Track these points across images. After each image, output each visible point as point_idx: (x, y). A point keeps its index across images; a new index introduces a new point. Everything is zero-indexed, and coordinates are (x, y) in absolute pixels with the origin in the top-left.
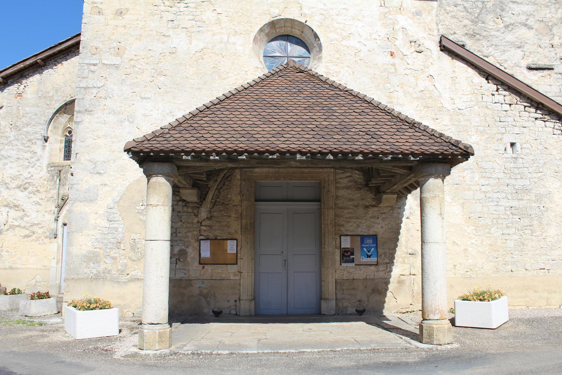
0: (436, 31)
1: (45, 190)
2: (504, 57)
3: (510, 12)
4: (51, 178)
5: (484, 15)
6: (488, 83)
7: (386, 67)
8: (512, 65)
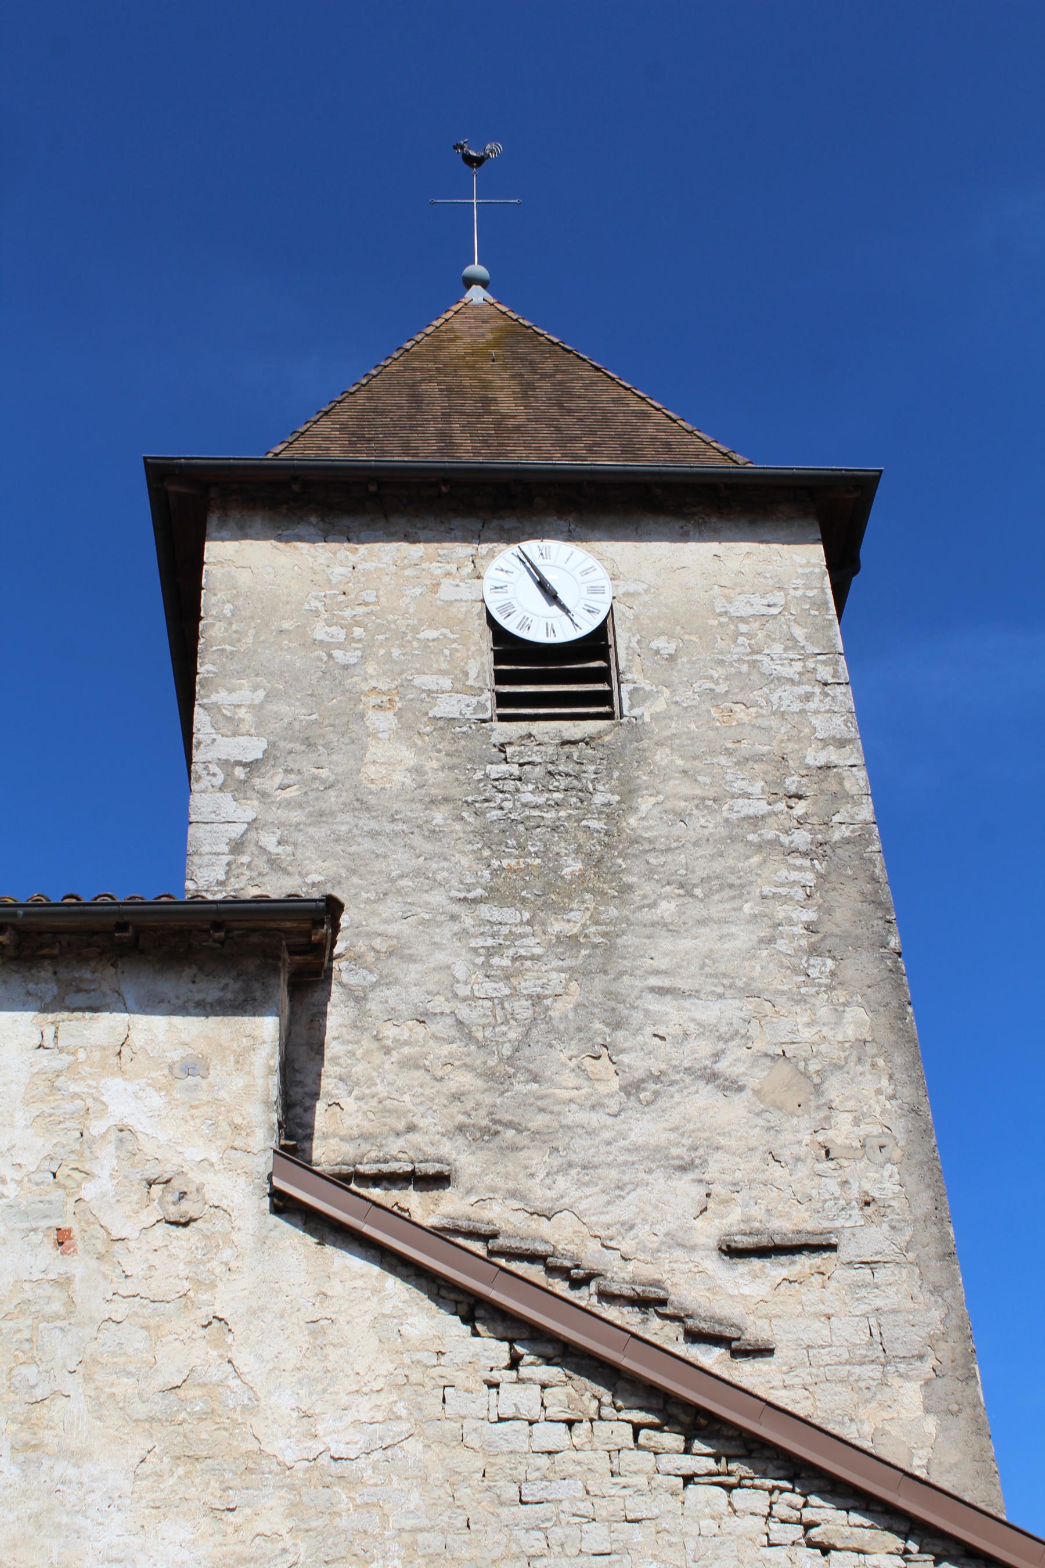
2: (622, 1211)
3: (649, 1030)
5: (536, 1048)
7: (29, 1295)
8: (654, 1242)
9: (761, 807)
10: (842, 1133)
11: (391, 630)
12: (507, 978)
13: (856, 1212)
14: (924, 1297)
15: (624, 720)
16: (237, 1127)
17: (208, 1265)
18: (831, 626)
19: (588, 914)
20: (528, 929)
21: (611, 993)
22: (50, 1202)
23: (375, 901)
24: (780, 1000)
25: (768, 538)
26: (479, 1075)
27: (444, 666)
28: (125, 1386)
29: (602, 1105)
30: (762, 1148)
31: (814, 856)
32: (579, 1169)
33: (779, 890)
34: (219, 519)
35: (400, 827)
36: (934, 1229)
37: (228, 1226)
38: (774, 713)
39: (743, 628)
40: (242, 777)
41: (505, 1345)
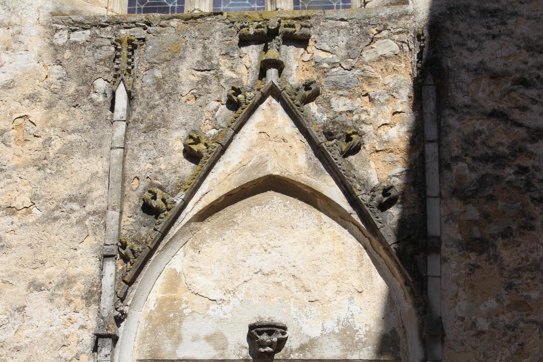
1: (27, 157)
4: (72, 88)
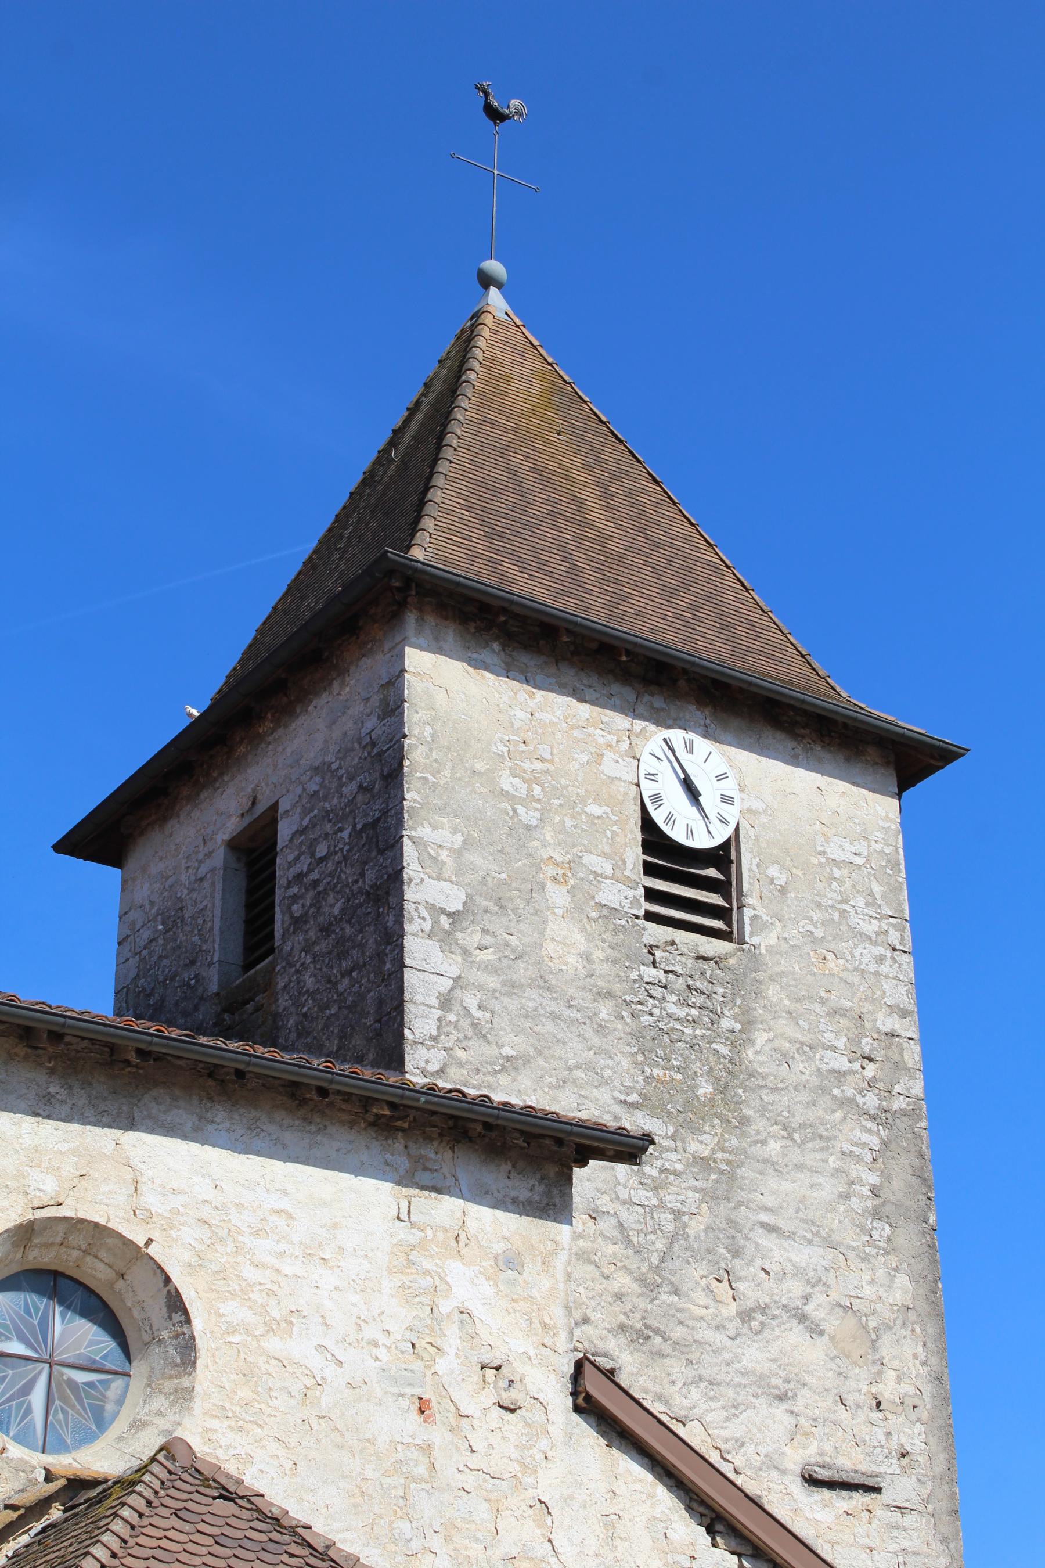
0: (563, 1335)
2: (735, 1429)
3: (758, 1263)
5: (678, 1263)
6: (714, 1545)
7: (400, 1456)
8: (757, 1461)
9: (841, 1063)
10: (888, 1390)
11: (564, 797)
12: (656, 1188)
13: (895, 1461)
14: (936, 1546)
15: (745, 946)
16: (546, 1326)
17: (531, 1451)
18: (901, 889)
19: (716, 1139)
20: (671, 1144)
21: (732, 1221)
22: (413, 1371)
23: (557, 1087)
24: (851, 1256)
25: (859, 780)
26: (636, 1280)
27: (607, 849)
28: (475, 1550)
29: (724, 1327)
30: (834, 1391)
31: (879, 1121)
32: (706, 1384)
33: (854, 1149)
34: (417, 620)
35: (575, 1014)
36: (946, 1487)
37: (544, 1417)
38: (856, 969)
39: (837, 873)
40: (447, 927)
41: (736, 1557)
